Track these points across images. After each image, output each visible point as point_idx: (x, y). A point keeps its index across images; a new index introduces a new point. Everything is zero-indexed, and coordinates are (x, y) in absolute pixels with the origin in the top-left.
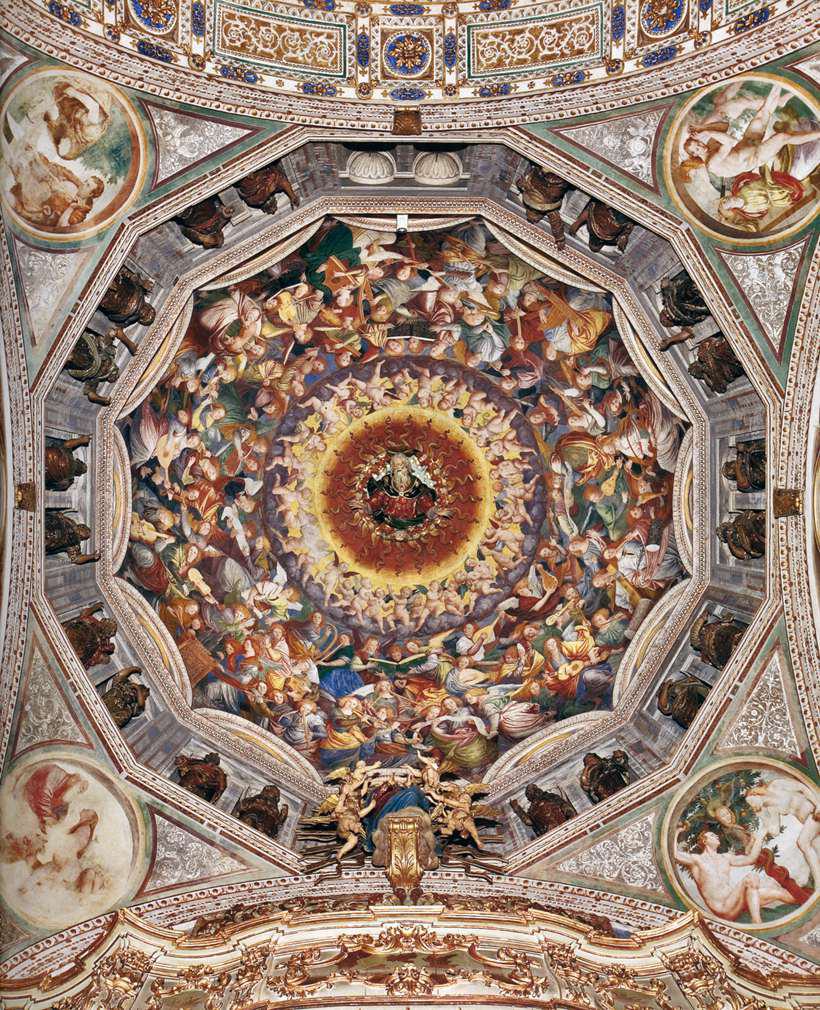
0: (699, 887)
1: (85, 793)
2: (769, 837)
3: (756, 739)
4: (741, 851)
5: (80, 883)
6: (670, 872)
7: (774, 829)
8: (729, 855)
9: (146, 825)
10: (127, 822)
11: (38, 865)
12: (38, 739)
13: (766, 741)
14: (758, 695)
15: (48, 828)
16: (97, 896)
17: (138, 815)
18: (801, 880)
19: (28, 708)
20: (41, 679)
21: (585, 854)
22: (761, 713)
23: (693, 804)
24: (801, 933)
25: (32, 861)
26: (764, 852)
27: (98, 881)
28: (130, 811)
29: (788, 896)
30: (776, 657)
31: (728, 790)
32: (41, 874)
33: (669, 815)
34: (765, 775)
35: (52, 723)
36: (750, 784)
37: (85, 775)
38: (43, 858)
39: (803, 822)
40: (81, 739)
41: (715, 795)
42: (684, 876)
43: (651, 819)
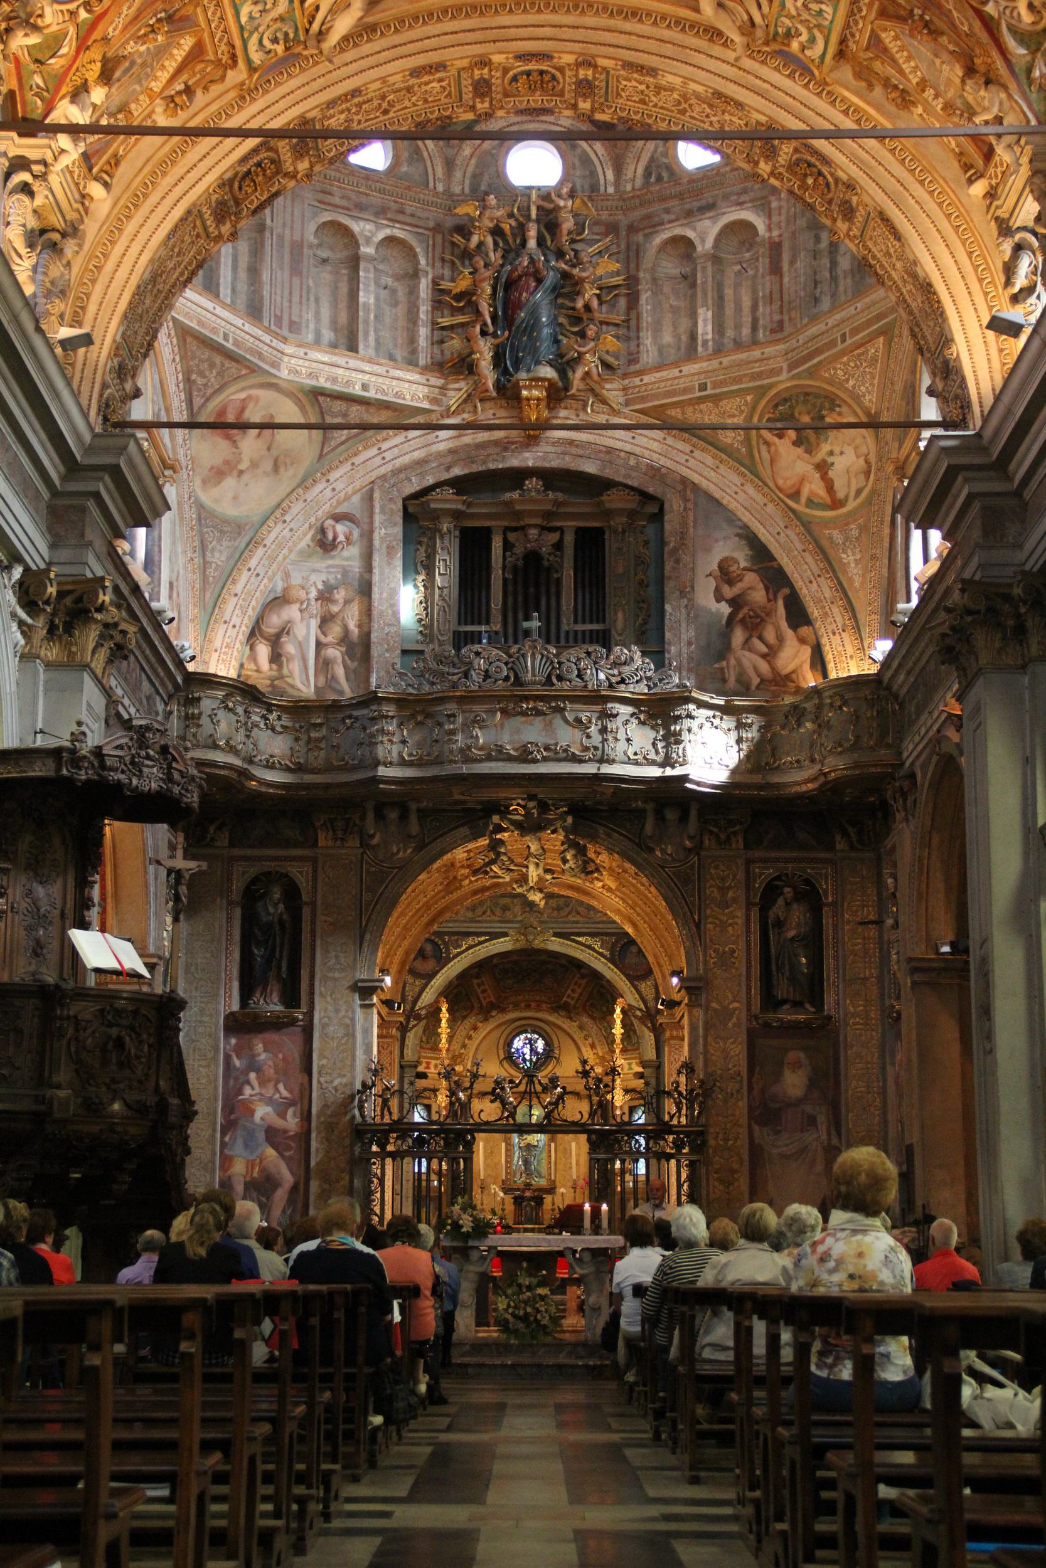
0: (772, 461)
1: (261, 404)
2: (831, 453)
3: (847, 381)
4: (809, 452)
5: (276, 468)
6: (754, 442)
7: (837, 450)
8: (800, 451)
9: (313, 406)
10: (296, 409)
11: (241, 472)
12: (210, 391)
13: (854, 387)
14: (859, 355)
15: (240, 444)
16: (290, 472)
17: (304, 400)
18: (840, 495)
19: (194, 377)
20: (198, 353)
21: (690, 409)
22: (856, 366)
23: (785, 400)
24: (827, 528)
25: (235, 473)
26: (824, 461)
27: (288, 461)
28: (298, 402)
29: (828, 500)
30: (881, 339)
31: (814, 405)
32: (246, 477)
33: (763, 402)
34: (844, 409)
35: (218, 374)
36: (832, 410)
37: (254, 392)
38: (243, 466)
39: (858, 457)
40: (244, 372)
41: (805, 402)
42: (764, 448)
43: (749, 398)
